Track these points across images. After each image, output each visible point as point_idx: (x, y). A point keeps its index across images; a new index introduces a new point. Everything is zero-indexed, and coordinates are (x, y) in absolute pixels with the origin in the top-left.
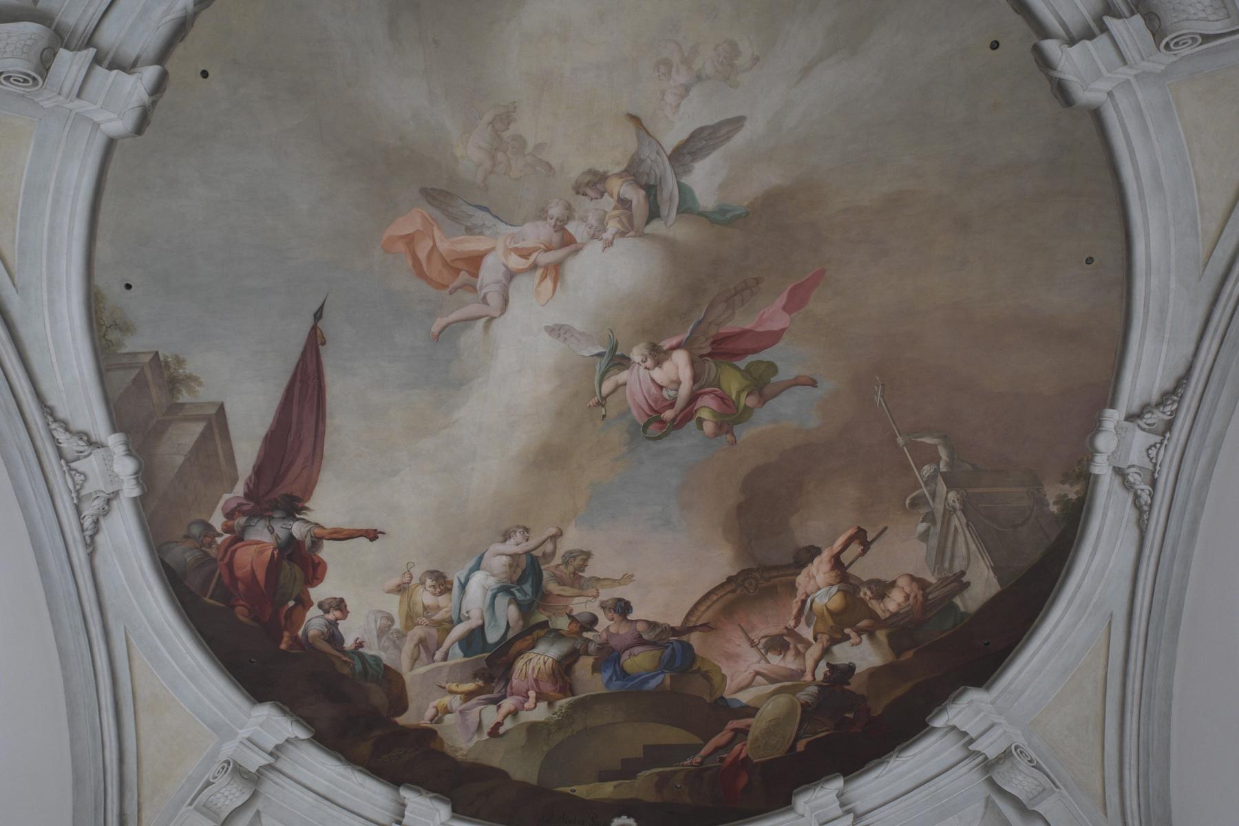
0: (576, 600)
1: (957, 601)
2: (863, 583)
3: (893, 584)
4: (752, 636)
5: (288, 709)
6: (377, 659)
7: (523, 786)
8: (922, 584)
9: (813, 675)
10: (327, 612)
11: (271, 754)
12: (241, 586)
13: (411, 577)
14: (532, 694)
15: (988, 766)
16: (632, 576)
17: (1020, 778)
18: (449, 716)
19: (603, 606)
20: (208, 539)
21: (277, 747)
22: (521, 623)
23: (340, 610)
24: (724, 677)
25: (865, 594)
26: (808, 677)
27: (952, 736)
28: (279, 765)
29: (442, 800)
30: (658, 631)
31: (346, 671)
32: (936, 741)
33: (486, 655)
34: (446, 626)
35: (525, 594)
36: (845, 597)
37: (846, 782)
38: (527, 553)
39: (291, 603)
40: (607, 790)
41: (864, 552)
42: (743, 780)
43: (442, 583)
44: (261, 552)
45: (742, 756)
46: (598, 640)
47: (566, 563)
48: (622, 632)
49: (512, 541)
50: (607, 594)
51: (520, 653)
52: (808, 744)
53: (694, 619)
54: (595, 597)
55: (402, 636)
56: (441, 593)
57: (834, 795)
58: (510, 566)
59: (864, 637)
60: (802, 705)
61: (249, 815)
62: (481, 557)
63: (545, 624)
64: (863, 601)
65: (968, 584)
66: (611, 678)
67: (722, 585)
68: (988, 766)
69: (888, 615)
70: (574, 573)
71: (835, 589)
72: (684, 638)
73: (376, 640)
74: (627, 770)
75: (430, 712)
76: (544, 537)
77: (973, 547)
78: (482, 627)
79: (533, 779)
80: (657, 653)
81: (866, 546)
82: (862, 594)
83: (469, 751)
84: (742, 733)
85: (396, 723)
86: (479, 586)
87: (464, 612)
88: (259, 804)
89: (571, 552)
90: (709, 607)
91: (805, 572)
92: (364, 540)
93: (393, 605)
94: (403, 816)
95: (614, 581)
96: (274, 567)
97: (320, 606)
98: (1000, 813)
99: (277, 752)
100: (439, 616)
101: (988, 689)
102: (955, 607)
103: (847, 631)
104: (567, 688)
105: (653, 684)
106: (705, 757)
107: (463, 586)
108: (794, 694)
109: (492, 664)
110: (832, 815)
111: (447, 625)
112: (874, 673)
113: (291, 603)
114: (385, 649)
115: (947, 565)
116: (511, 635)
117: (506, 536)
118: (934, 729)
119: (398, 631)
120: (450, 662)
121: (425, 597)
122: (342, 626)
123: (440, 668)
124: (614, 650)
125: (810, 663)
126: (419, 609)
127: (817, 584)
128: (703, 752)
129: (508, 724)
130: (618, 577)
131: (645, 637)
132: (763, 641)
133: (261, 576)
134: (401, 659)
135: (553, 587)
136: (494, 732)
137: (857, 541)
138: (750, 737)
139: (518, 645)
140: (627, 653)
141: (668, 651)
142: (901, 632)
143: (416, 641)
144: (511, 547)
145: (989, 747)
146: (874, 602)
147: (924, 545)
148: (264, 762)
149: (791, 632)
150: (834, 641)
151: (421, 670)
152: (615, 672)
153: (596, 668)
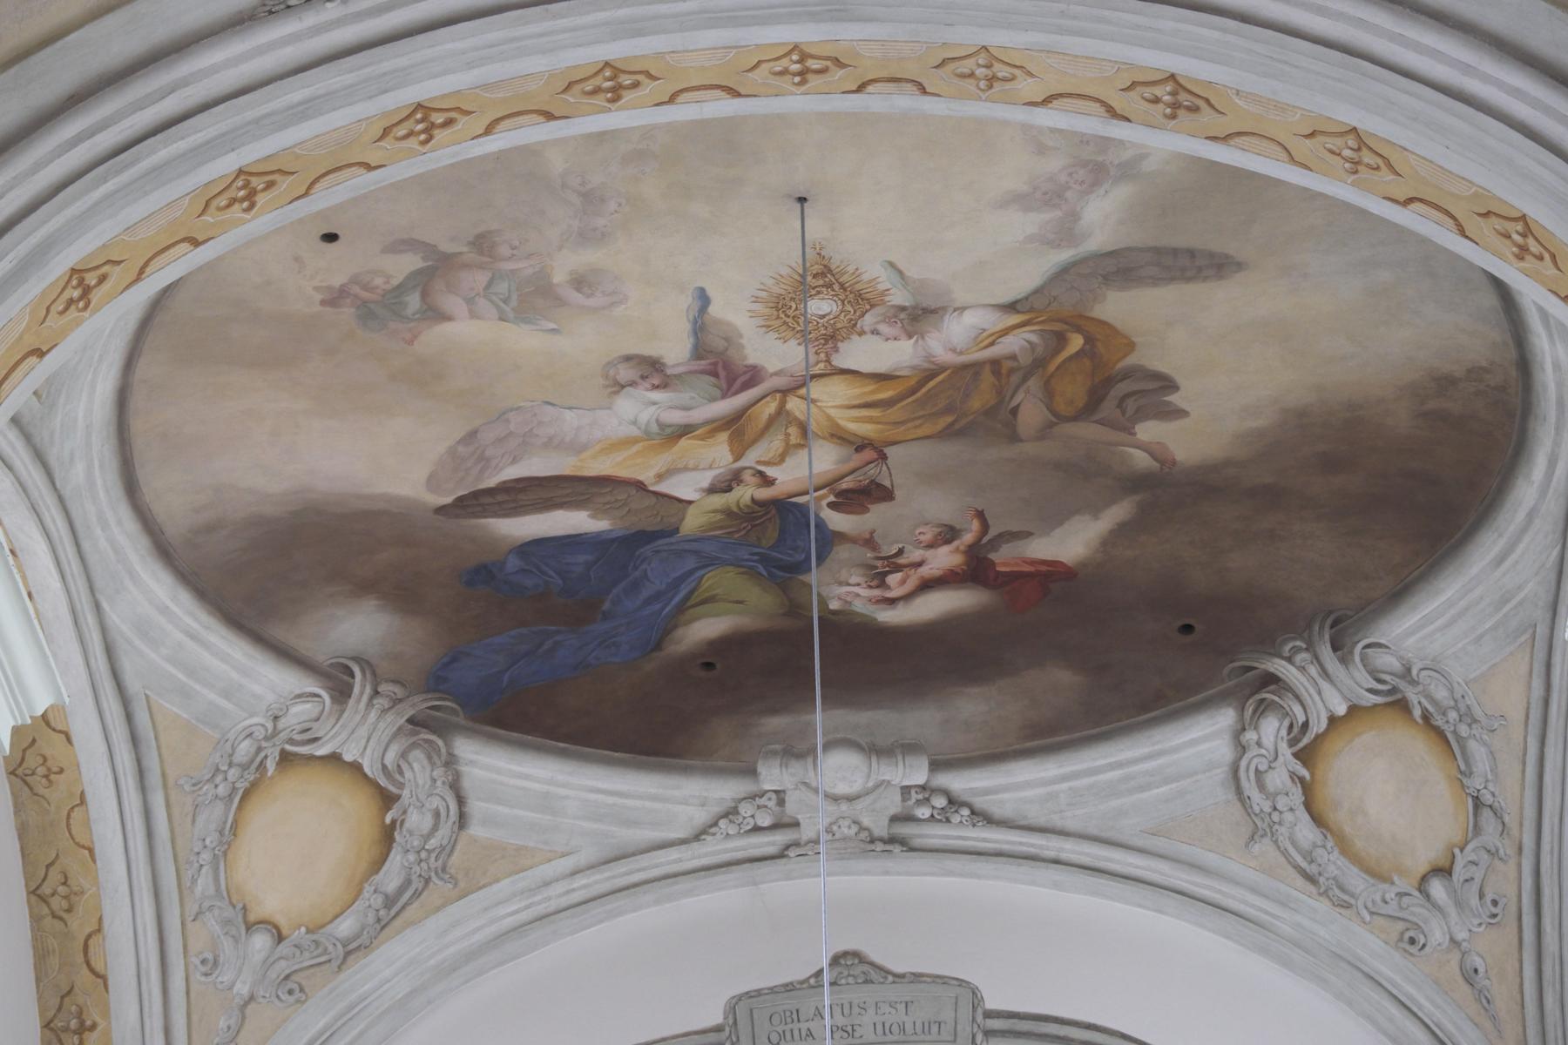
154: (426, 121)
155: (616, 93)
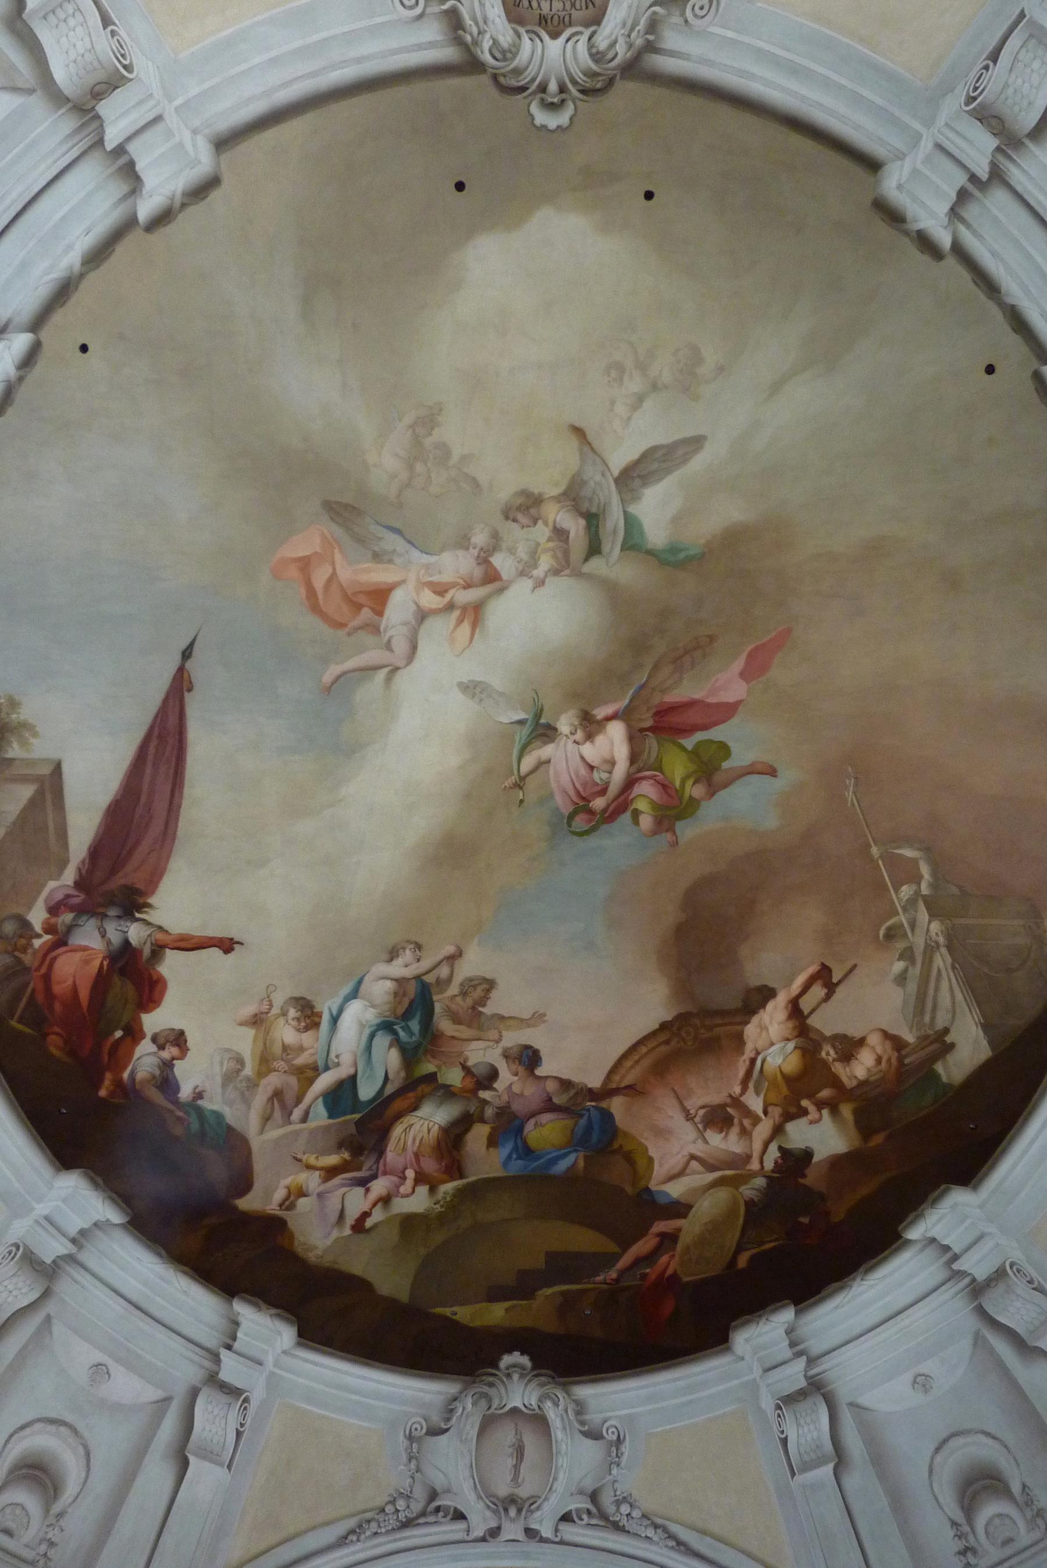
0: (475, 1045)
1: (939, 1067)
2: (825, 1039)
3: (861, 1042)
4: (688, 1104)
5: (100, 1181)
6: (219, 1116)
7: (391, 1303)
8: (896, 1042)
9: (761, 1162)
10: (162, 1047)
11: (74, 1241)
12: (58, 1007)
13: (271, 1005)
14: (410, 1174)
15: (977, 1290)
16: (544, 1015)
17: (1018, 1304)
18: (302, 1201)
19: (506, 1055)
20: (23, 941)
21: (83, 1232)
22: (403, 1074)
23: (178, 1045)
24: (651, 1160)
25: (828, 1053)
26: (755, 1165)
27: (930, 1252)
28: (82, 1257)
29: (287, 1320)
30: (572, 1092)
31: (178, 1131)
32: (911, 1259)
33: (357, 1116)
34: (308, 1074)
35: (411, 1034)
36: (804, 1055)
37: (797, 1313)
38: (418, 978)
39: (119, 1034)
41: (828, 997)
42: (668, 1306)
43: (308, 1015)
44: (87, 962)
45: (669, 1272)
46: (497, 1102)
47: (464, 994)
48: (527, 1092)
49: (399, 961)
50: (513, 1038)
51: (399, 1116)
52: (752, 1259)
53: (617, 1078)
54: (497, 1042)
55: (253, 1085)
56: (307, 1029)
57: (781, 1332)
58: (396, 994)
59: (825, 1112)
60: (746, 1203)
61: (35, 1321)
62: (360, 982)
63: (432, 1078)
64: (825, 1064)
65: (952, 1046)
66: (509, 1157)
67: (653, 1034)
68: (977, 1290)
69: (854, 1083)
70: (473, 1008)
71: (791, 1045)
72: (604, 1104)
73: (219, 1090)
74: (522, 1287)
75: (280, 1194)
76: (440, 957)
77: (959, 996)
78: (353, 1079)
79: (403, 1296)
80: (569, 1122)
81: (831, 988)
82: (823, 1054)
84: (669, 1239)
85: (235, 1208)
86: (356, 1018)
87: (332, 1056)
88: (51, 1307)
89: (471, 980)
90: (637, 1062)
91: (755, 1020)
92: (215, 952)
93: (245, 1042)
94: (234, 1338)
95: (522, 1020)
96: (101, 982)
97: (154, 1039)
98: (992, 1351)
99: (80, 1239)
100: (301, 1060)
101: (975, 1188)
102: (936, 1076)
103: (805, 1103)
104: (454, 1168)
105: (562, 1166)
106: (622, 1273)
107: (335, 1020)
108: (737, 1189)
109: (363, 1129)
110: (780, 1358)
111: (310, 1073)
112: (837, 1162)
113: (119, 1034)
114: (230, 1104)
115: (927, 1019)
116: (389, 1090)
117: (393, 954)
118: (908, 1242)
119: (248, 1079)
120: (312, 1124)
121: (286, 1033)
122: (180, 1069)
123: (297, 1133)
124: (516, 1117)
125: (757, 1146)
126: (277, 1049)
127: (770, 1040)
129: (378, 1216)
130: (526, 1015)
131: (556, 1100)
132: (701, 1112)
133: (84, 994)
134: (246, 1117)
135: (445, 1025)
136: (359, 1226)
137: (819, 983)
138: (680, 1246)
139: (398, 1105)
140: (532, 1121)
141: (583, 1122)
142: (871, 1107)
143: (270, 1093)
144: (398, 969)
145: (978, 1264)
146: (838, 1065)
147: (900, 990)
148: (62, 1251)
149: (736, 1102)
150: (788, 1117)
151: (274, 1133)
152: (515, 1149)
153: (492, 1142)
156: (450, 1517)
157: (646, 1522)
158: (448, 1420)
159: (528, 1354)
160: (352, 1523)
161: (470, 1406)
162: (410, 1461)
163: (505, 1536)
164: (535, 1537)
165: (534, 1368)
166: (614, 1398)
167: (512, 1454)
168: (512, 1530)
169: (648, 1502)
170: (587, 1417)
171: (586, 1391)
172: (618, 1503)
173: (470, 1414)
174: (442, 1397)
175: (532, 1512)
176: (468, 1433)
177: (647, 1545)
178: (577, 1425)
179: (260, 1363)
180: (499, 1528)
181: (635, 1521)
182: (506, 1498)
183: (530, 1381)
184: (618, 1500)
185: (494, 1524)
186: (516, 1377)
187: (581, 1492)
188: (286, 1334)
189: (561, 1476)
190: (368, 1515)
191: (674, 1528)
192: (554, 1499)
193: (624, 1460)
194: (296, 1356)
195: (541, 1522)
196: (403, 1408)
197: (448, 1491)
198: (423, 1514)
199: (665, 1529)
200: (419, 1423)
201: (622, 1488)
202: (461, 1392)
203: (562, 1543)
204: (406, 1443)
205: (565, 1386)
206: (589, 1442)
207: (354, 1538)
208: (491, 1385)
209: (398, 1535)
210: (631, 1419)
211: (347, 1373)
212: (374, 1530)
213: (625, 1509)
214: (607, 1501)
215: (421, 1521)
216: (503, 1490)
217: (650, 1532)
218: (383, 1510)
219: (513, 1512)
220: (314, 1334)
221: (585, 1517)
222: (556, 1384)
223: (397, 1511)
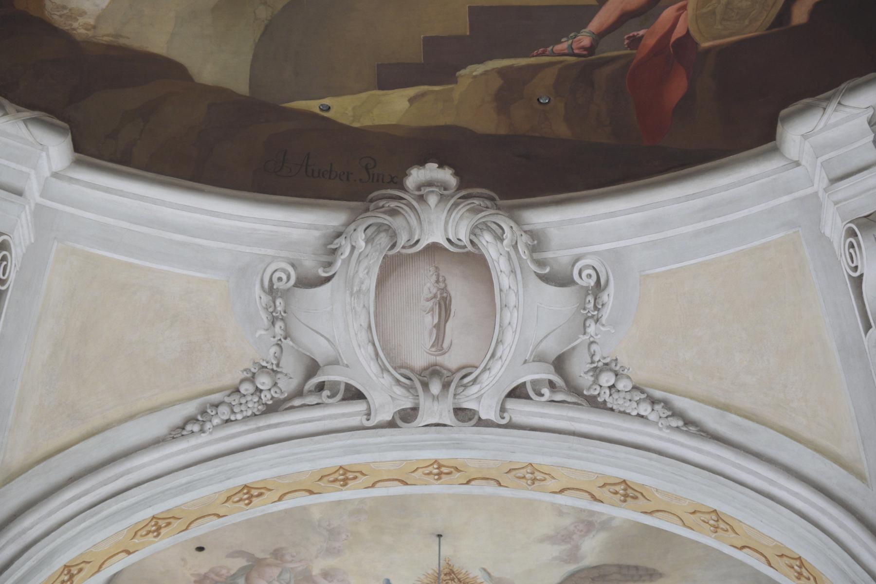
7: (218, 95)
40: (395, 107)
42: (678, 87)
57: (862, 122)
74: (436, 63)
79: (241, 86)
83: (99, 18)
106: (600, 36)
128: (597, 23)
154: (249, 494)
155: (345, 482)
156: (340, 396)
157: (638, 396)
158: (330, 264)
159: (451, 166)
160: (191, 408)
161: (363, 244)
162: (273, 323)
163: (424, 418)
164: (470, 419)
165: (460, 188)
166: (591, 227)
167: (432, 309)
168: (436, 409)
169: (641, 369)
170: (549, 255)
171: (546, 218)
172: (596, 372)
173: (363, 256)
174: (317, 233)
175: (465, 386)
176: (362, 283)
177: (637, 426)
178: (533, 267)
179: (19, 193)
180: (415, 409)
181: (622, 395)
182: (425, 369)
183: (456, 205)
184: (596, 368)
185: (408, 404)
186: (432, 200)
187: (540, 358)
188: (54, 149)
189: (509, 337)
190: (215, 398)
191: (680, 402)
192: (497, 368)
193: (606, 313)
194: (77, 181)
195: (479, 399)
196: (256, 250)
197: (335, 362)
198: (299, 393)
199: (667, 404)
200: (284, 270)
201: (602, 353)
202: (347, 225)
203: (510, 426)
204: (266, 299)
205: (511, 212)
206: (551, 290)
207: (196, 428)
208: (393, 213)
209: (262, 422)
210: (617, 256)
211: (163, 203)
212: (225, 417)
213: (607, 379)
214: (580, 368)
215: (297, 402)
216: (420, 359)
217: (645, 409)
218: (238, 391)
219: (435, 387)
220: (98, 147)
221: (546, 391)
222: (499, 208)
223: (258, 391)
